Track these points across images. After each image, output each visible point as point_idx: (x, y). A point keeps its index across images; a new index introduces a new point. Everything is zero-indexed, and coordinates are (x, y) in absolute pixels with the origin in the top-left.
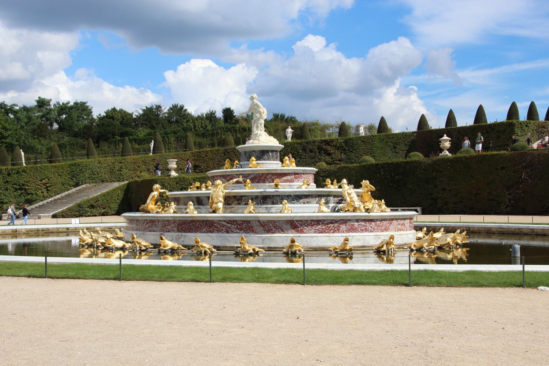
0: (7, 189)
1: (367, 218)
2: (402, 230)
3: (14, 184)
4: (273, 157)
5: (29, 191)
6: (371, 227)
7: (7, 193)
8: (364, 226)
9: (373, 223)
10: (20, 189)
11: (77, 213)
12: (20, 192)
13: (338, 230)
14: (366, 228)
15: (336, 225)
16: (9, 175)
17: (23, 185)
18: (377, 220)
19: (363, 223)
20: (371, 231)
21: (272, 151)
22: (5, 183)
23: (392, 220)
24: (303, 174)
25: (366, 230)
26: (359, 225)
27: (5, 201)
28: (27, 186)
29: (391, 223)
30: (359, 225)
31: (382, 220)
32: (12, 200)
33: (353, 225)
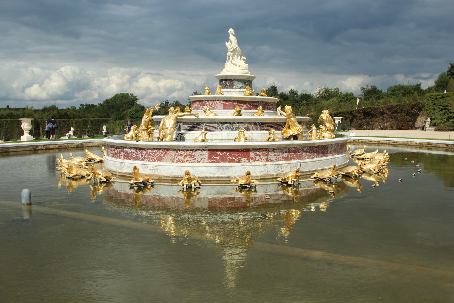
0: (434, 109)
1: (136, 147)
2: (187, 161)
3: (440, 106)
4: (226, 85)
5: (451, 111)
6: (142, 156)
7: (434, 112)
8: (136, 154)
9: (144, 153)
10: (445, 109)
11: (450, 128)
12: (444, 111)
13: (119, 156)
14: (137, 156)
15: (118, 150)
16: (436, 99)
17: (447, 106)
18: (148, 149)
19: (134, 151)
20: (142, 160)
21: (225, 80)
22: (433, 105)
23: (168, 150)
24: (208, 101)
25: (138, 158)
26: (132, 152)
27: (434, 117)
28: (450, 107)
29: (166, 153)
30: (132, 152)
31: (154, 149)
32: (438, 117)
33: (127, 152)
